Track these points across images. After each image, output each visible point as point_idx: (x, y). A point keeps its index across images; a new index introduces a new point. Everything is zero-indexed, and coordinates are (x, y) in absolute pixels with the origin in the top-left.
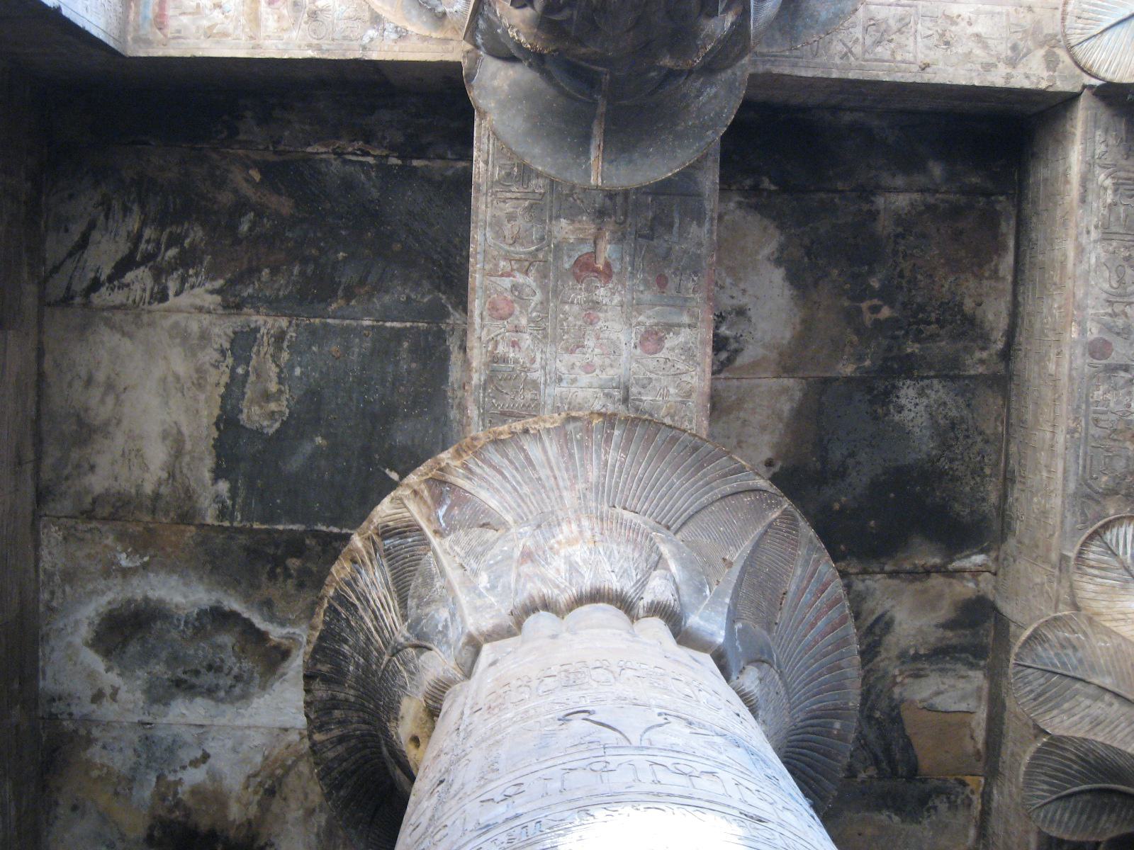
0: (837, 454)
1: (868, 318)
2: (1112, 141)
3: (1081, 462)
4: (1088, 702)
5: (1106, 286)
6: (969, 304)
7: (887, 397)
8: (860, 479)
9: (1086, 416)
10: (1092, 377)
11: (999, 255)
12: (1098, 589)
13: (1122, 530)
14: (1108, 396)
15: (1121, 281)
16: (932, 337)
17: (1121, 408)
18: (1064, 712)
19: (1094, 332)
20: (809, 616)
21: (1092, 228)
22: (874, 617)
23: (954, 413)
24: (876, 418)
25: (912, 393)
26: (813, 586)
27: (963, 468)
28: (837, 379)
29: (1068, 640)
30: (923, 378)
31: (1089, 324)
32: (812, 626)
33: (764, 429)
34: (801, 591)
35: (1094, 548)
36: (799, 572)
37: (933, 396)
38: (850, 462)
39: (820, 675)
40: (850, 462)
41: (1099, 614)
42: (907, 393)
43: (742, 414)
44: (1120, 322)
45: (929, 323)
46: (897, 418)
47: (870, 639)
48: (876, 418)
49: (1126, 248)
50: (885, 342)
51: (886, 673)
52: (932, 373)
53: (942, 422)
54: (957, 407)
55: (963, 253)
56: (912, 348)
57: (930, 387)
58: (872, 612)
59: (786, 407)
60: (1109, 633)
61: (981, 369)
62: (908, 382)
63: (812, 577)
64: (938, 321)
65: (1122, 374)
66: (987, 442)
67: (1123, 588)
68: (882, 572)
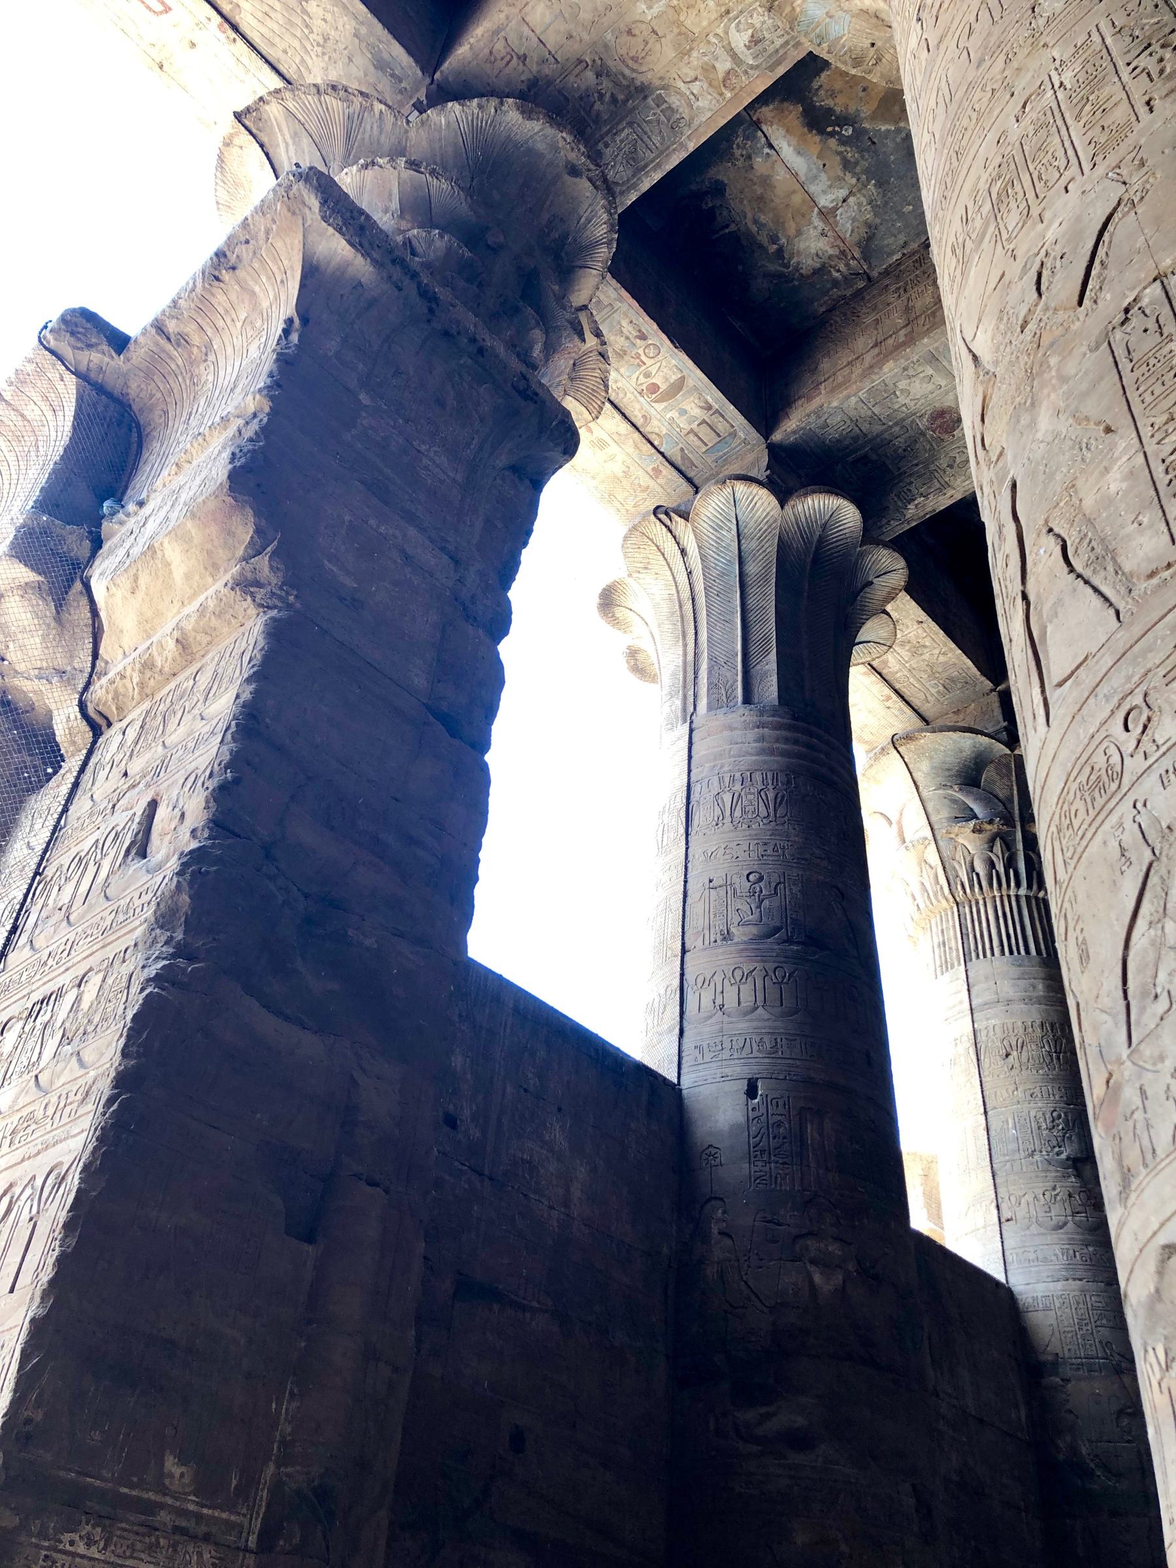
2: (884, 521)
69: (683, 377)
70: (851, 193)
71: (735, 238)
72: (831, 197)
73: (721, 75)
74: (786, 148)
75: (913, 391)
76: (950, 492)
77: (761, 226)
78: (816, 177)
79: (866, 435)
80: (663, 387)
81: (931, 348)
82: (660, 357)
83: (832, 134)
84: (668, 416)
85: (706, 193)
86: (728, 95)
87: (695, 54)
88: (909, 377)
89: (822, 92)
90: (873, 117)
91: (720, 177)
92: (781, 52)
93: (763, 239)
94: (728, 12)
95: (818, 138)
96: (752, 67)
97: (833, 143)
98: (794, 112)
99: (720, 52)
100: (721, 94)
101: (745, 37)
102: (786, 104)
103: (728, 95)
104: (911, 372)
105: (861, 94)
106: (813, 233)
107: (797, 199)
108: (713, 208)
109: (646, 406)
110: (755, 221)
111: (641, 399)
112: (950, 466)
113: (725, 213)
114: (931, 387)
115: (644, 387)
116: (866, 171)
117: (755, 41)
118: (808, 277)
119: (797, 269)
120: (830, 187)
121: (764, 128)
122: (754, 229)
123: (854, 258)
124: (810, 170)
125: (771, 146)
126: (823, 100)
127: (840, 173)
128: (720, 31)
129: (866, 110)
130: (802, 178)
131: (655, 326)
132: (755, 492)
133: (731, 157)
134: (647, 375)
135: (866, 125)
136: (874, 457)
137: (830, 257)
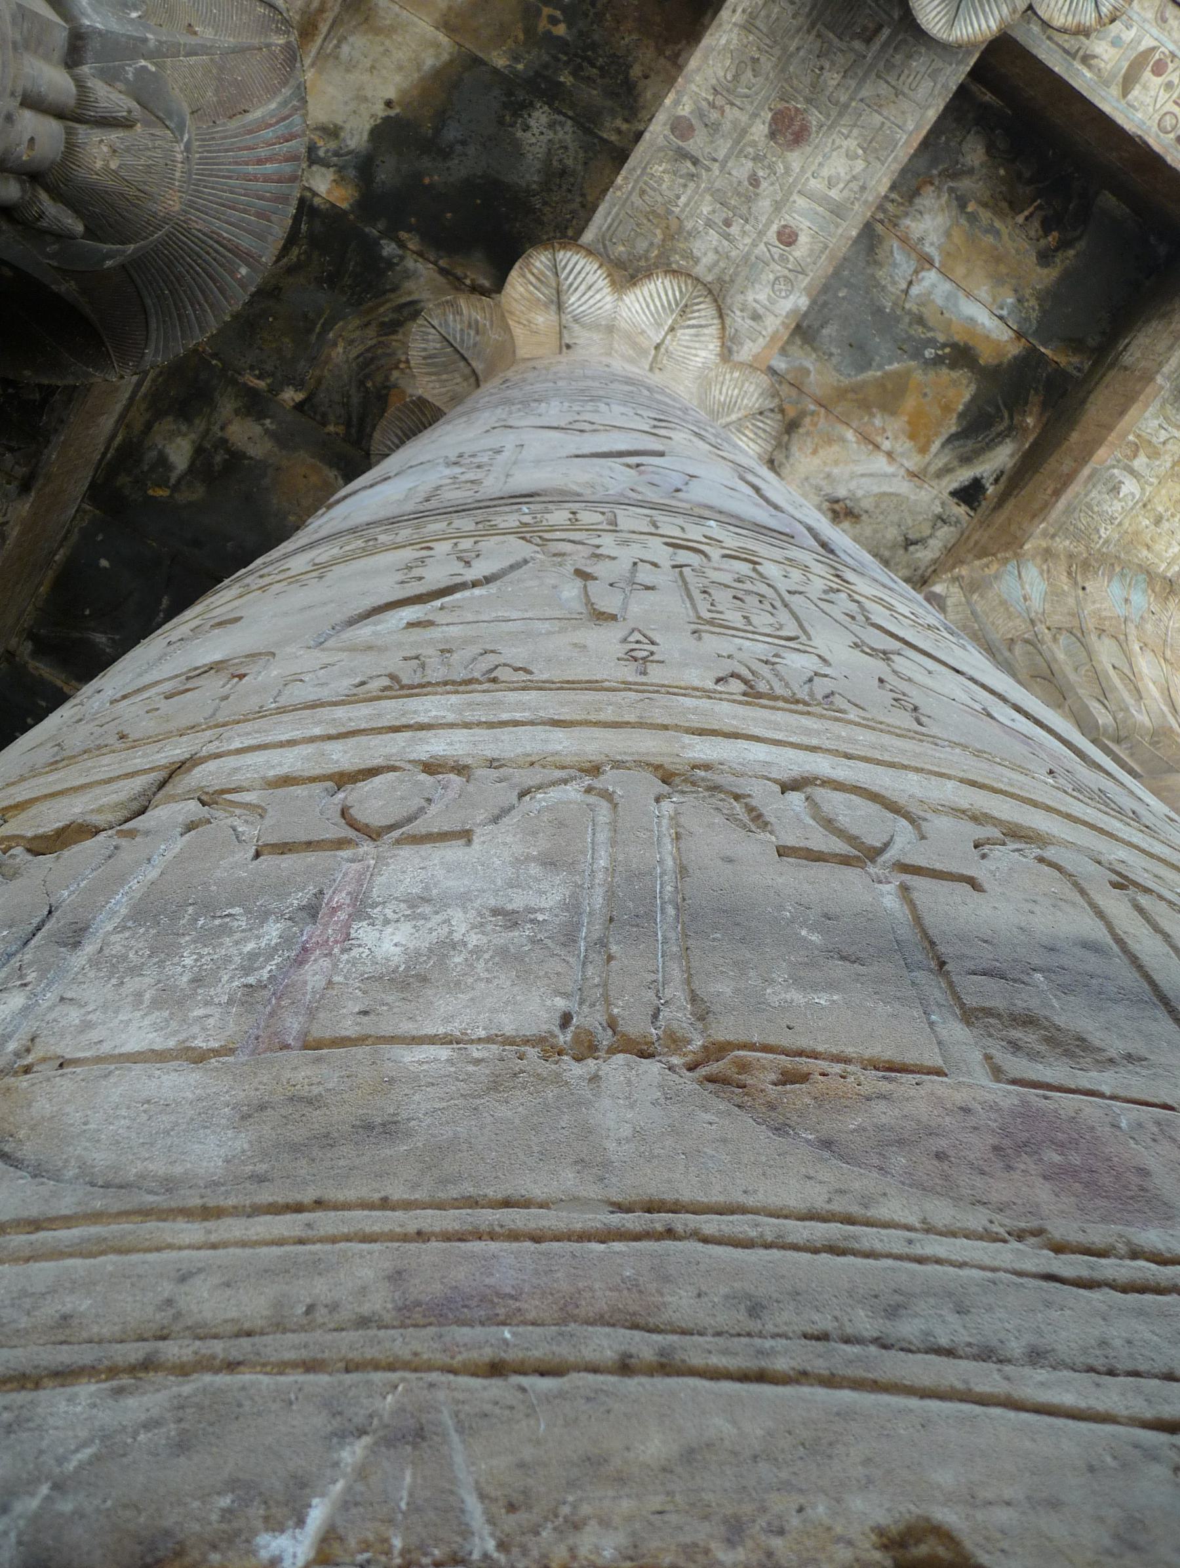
0: (451, 133)
1: (543, 25)
3: (609, 220)
4: (459, 380)
5: (721, 73)
6: (636, 71)
7: (520, 108)
8: (461, 168)
9: (636, 181)
10: (661, 149)
11: (688, 43)
12: (526, 294)
13: (575, 258)
14: (666, 176)
15: (736, 77)
16: (589, 80)
17: (671, 195)
18: (440, 381)
19: (685, 110)
20: (263, 152)
21: (740, 10)
22: (409, 299)
23: (569, 162)
24: (501, 122)
25: (544, 119)
26: (281, 129)
27: (551, 216)
28: (485, 64)
29: (477, 321)
30: (560, 113)
31: (685, 99)
32: (260, 162)
33: (400, 68)
34: (265, 125)
35: (543, 259)
36: (273, 106)
37: (561, 134)
38: (459, 148)
39: (245, 211)
40: (459, 148)
41: (511, 313)
42: (540, 117)
43: (387, 42)
44: (714, 115)
45: (593, 65)
46: (519, 134)
47: (395, 316)
48: (501, 122)
49: (759, 49)
50: (546, 58)
51: (394, 353)
52: (570, 113)
53: (555, 163)
54: (575, 158)
55: (658, 19)
56: (566, 78)
57: (562, 124)
58: (410, 293)
59: (430, 61)
60: (507, 329)
61: (613, 138)
62: (546, 108)
63: (284, 119)
64: (601, 68)
65: (689, 164)
66: (583, 206)
67: (546, 306)
68: (435, 263)
69: (1125, 95)
70: (906, 292)
71: (1015, 206)
72: (926, 283)
73: (1142, 453)
74: (985, 320)
75: (843, 160)
76: (738, 17)
77: (991, 230)
78: (947, 298)
79: (879, 76)
80: (1147, 74)
81: (845, 224)
82: (1157, 117)
83: (944, 346)
84: (1134, 31)
85: (1057, 249)
86: (1131, 438)
87: (1169, 465)
88: (854, 178)
89: (965, 382)
90: (908, 373)
91: (1046, 271)
92: (1090, 486)
93: (985, 215)
94: (1145, 506)
95: (957, 338)
96: (1114, 467)
97: (941, 338)
98: (986, 357)
99: (1145, 472)
100: (1138, 436)
101: (1124, 490)
102: (996, 362)
103: (1131, 438)
104: (855, 186)
105: (927, 390)
106: (933, 237)
107: (960, 271)
108: (1046, 233)
109: (1164, 38)
110: (997, 233)
111: (1172, 47)
112: (755, 61)
113: (1032, 233)
114: (825, 172)
115: (1171, 66)
116: (898, 320)
117: (1115, 489)
118: (925, 183)
119: (939, 189)
120: (930, 293)
121: (1011, 333)
122: (998, 224)
123: (881, 222)
124: (956, 305)
125: (1001, 318)
126: (961, 375)
127: (922, 309)
128: (1148, 489)
129: (918, 376)
130: (961, 294)
131: (1169, 159)
132: (1070, 18)
133: (1042, 297)
134: (1169, 86)
135: (913, 363)
136: (857, 45)
137: (906, 214)
